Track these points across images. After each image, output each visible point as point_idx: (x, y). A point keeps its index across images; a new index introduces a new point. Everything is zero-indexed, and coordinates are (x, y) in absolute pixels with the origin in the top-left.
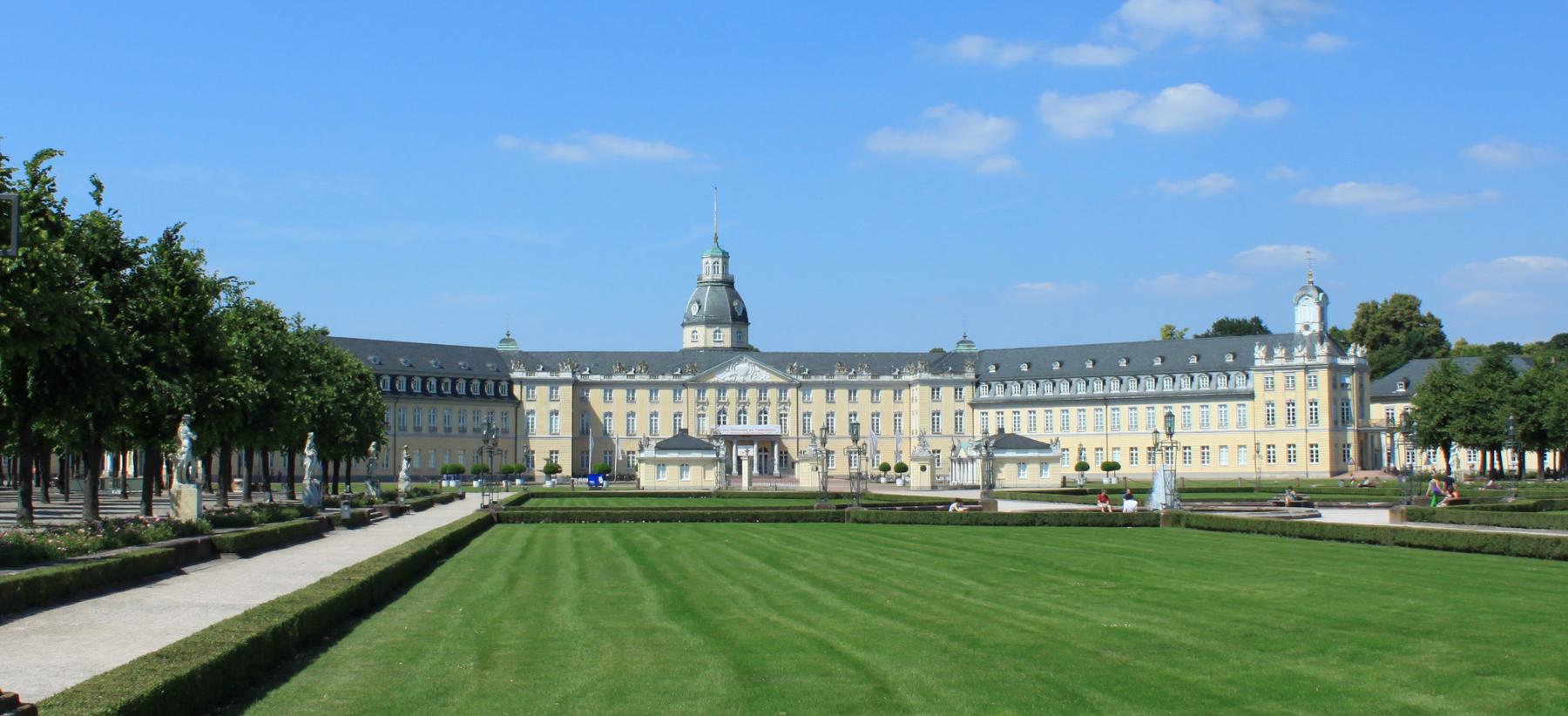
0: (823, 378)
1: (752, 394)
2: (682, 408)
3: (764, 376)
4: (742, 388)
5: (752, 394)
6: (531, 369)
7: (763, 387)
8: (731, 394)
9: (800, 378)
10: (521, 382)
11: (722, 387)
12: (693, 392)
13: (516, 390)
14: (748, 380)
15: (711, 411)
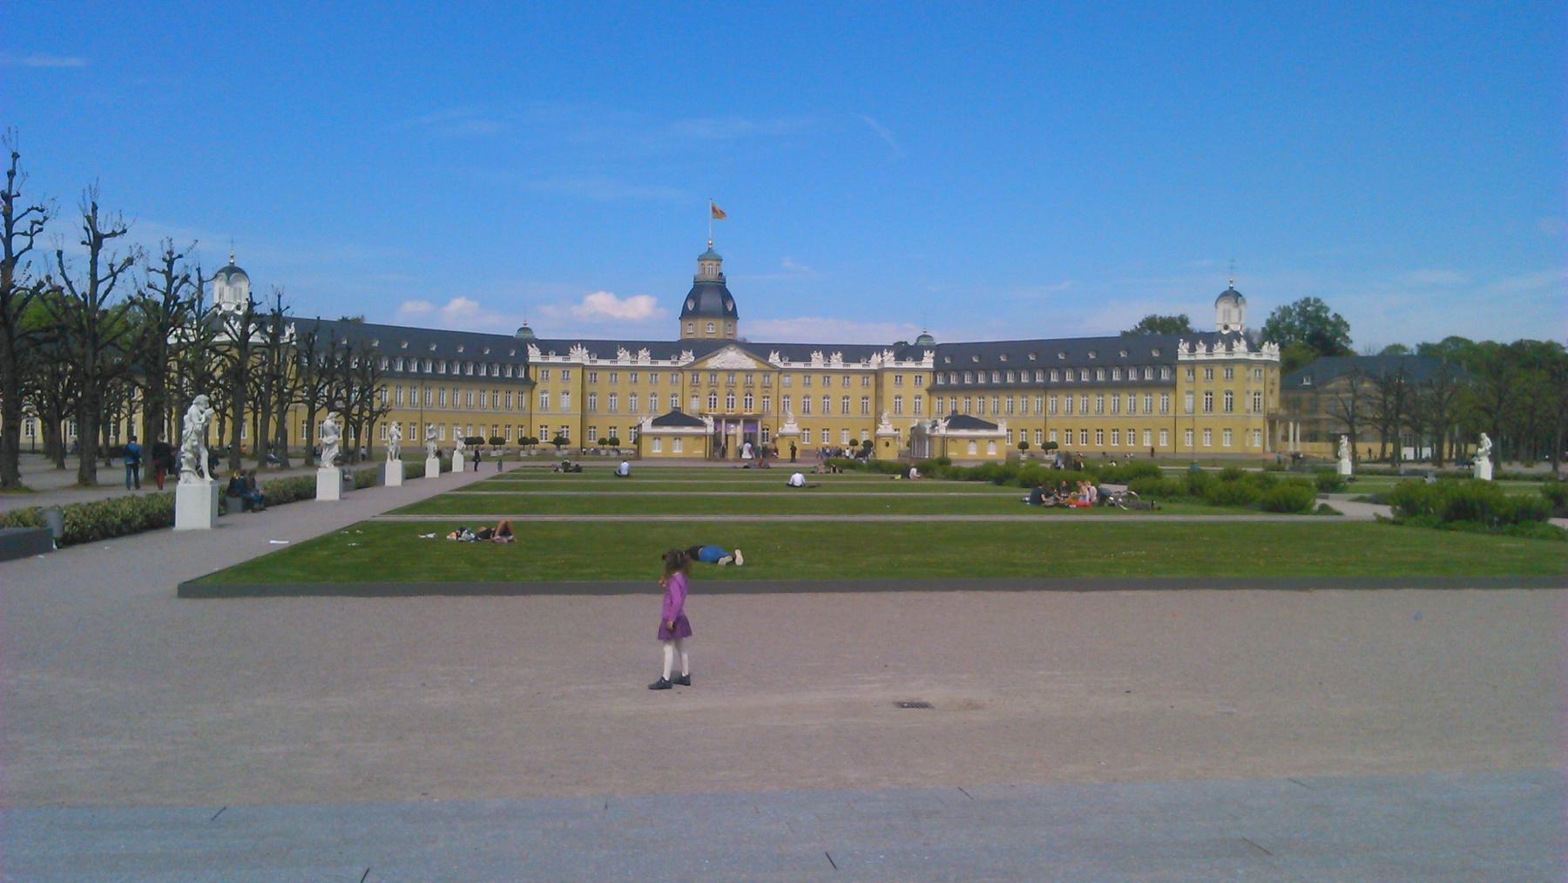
0: (800, 365)
1: (740, 379)
2: (678, 390)
3: (750, 363)
4: (731, 372)
5: (740, 379)
6: (545, 353)
7: (748, 372)
8: (722, 378)
9: (782, 366)
10: (536, 365)
11: (714, 372)
12: (688, 376)
13: (532, 370)
14: (735, 366)
15: (704, 391)
